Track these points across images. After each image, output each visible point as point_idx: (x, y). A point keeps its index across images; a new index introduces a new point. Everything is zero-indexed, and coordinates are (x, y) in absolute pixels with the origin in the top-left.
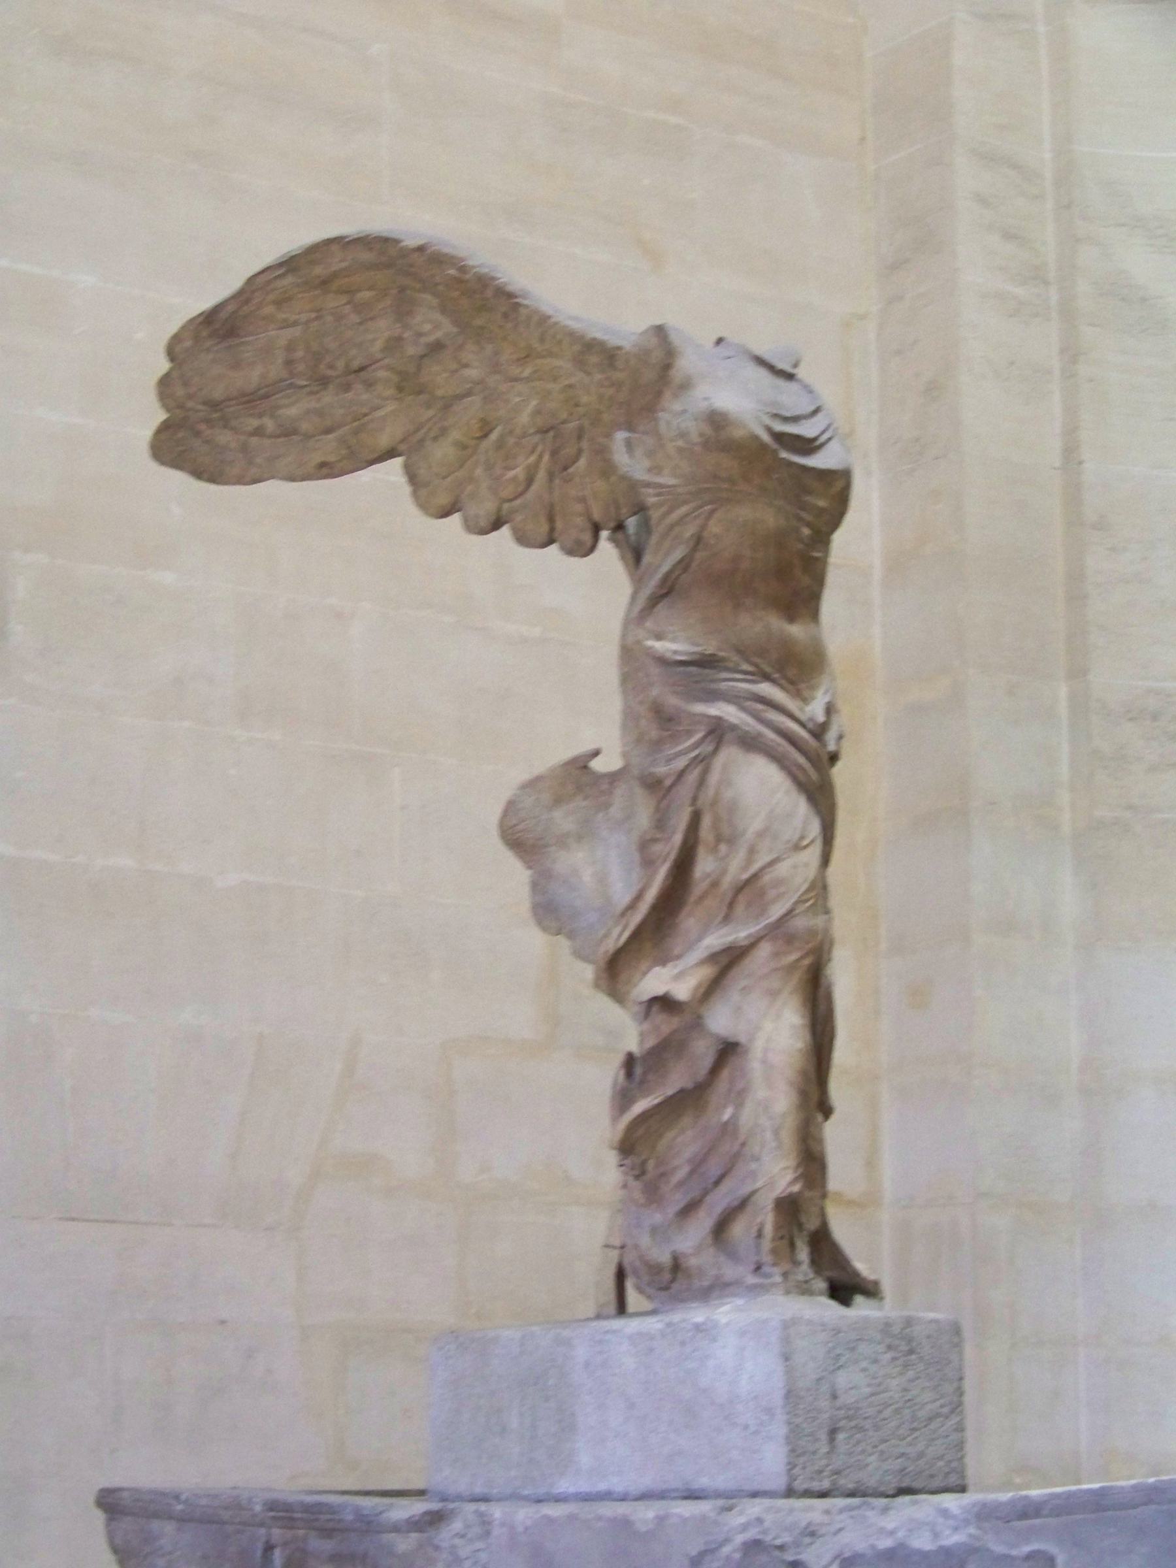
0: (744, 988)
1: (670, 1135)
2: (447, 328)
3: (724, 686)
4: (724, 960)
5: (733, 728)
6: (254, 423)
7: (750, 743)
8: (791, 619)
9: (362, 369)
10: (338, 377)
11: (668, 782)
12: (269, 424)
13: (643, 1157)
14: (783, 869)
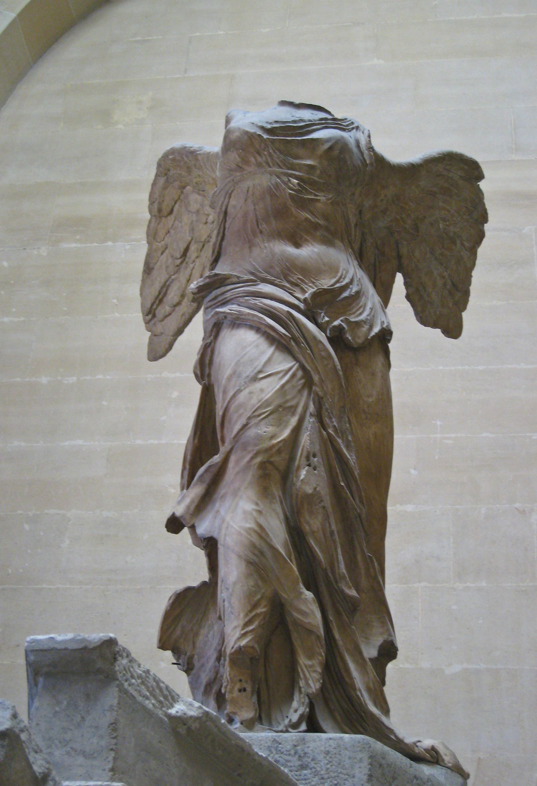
0: (222, 497)
1: (203, 632)
2: (199, 198)
4: (208, 478)
5: (225, 316)
6: (163, 311)
7: (237, 322)
8: (297, 245)
9: (187, 250)
10: (182, 263)
11: (198, 372)
12: (168, 309)
13: (188, 654)
14: (241, 397)
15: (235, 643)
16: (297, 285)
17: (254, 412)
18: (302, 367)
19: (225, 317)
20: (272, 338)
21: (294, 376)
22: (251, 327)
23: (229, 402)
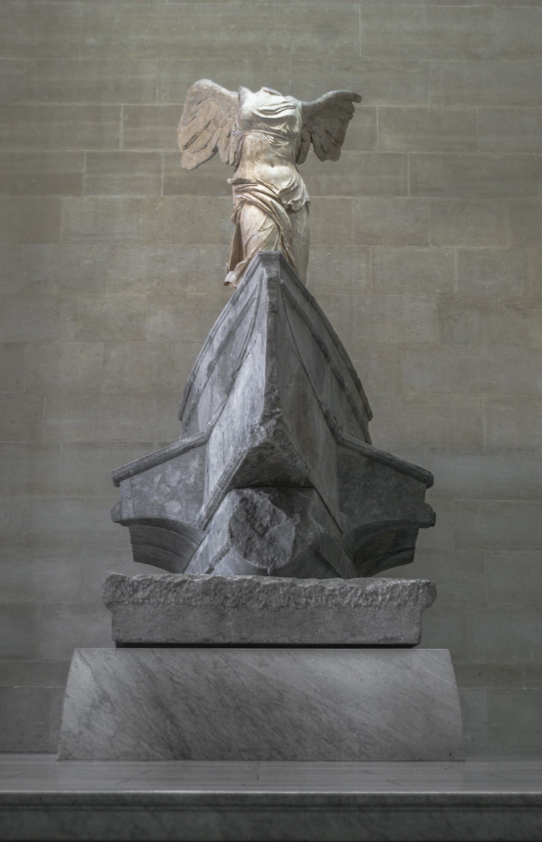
3: (246, 188)
4: (242, 268)
7: (251, 203)
14: (254, 238)
16: (273, 185)
18: (276, 223)
20: (265, 212)
21: (274, 228)
22: (257, 206)
23: (249, 239)
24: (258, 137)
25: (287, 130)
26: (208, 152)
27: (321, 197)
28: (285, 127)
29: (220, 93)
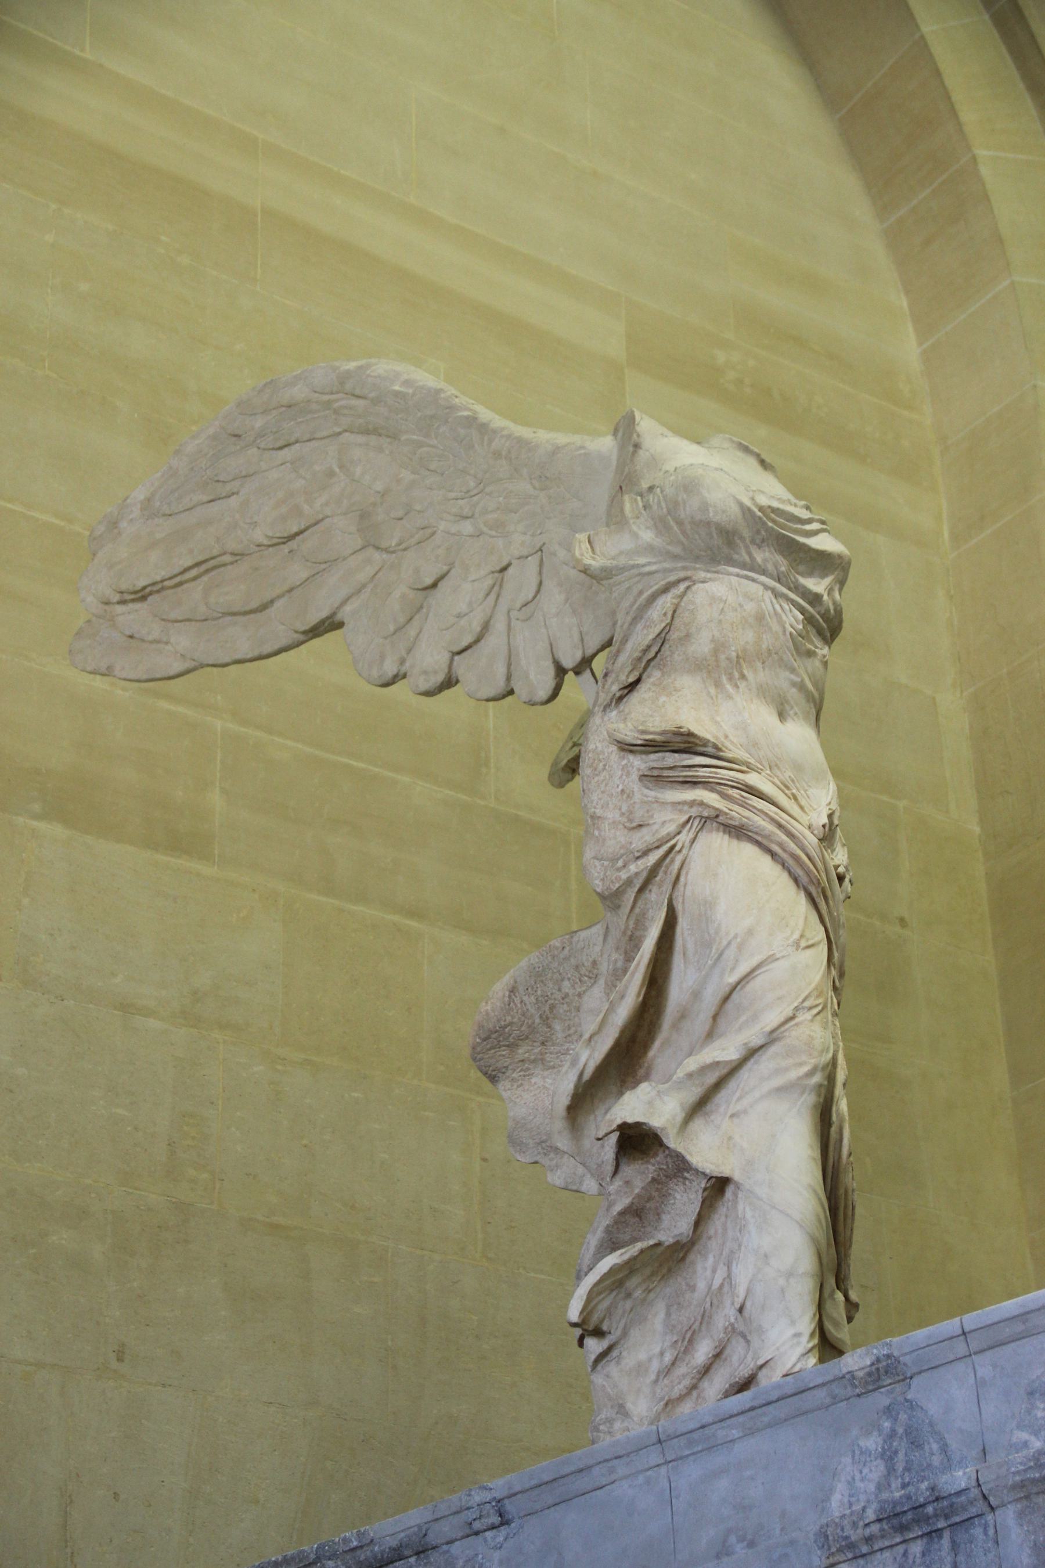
0: (732, 1116)
3: (702, 772)
4: (711, 1079)
7: (738, 831)
14: (778, 970)
15: (799, 1360)
17: (804, 1001)
19: (717, 816)
20: (796, 880)
24: (747, 596)
25: (834, 603)
26: (279, 625)
27: (336, 902)
28: (830, 591)
29: (472, 421)
